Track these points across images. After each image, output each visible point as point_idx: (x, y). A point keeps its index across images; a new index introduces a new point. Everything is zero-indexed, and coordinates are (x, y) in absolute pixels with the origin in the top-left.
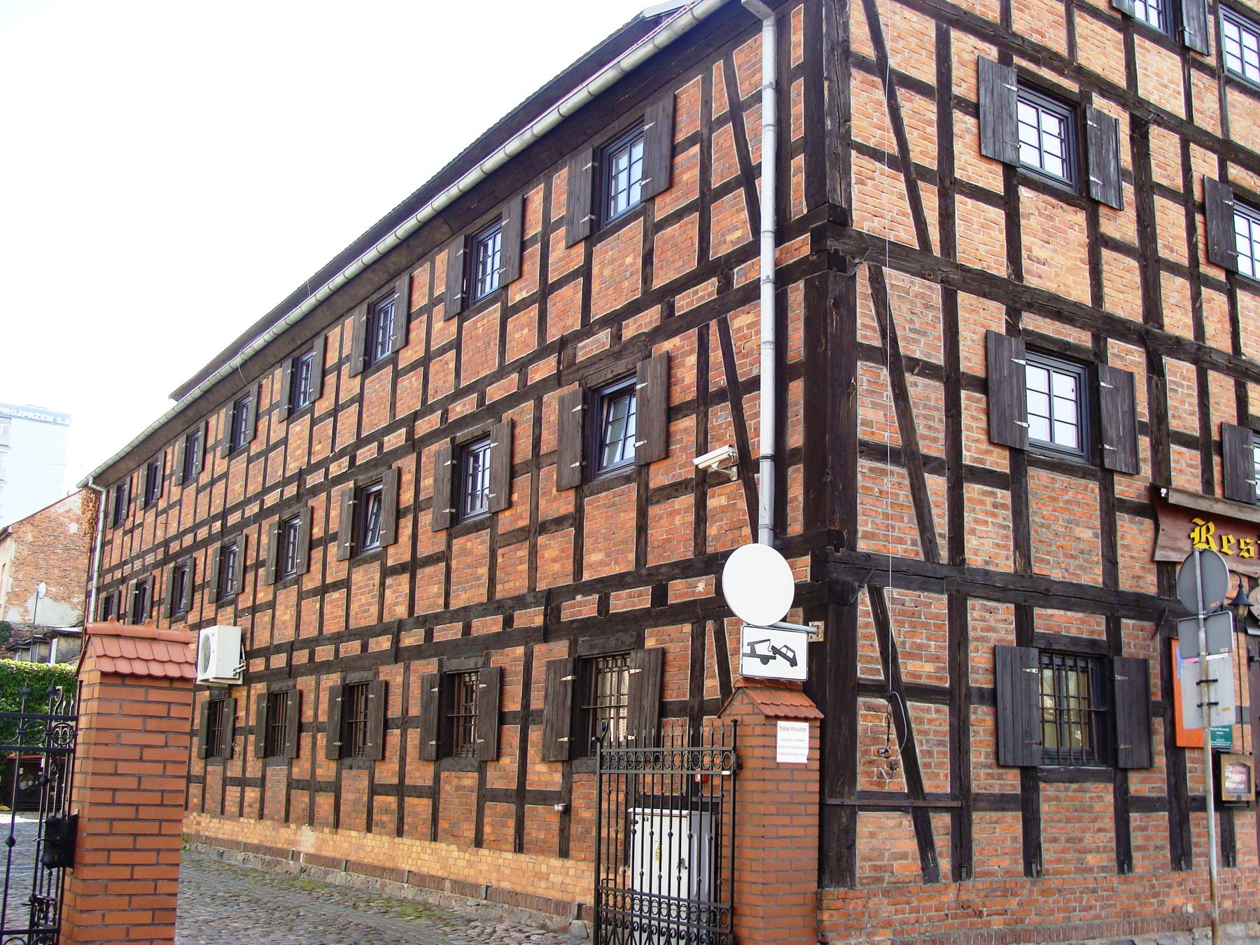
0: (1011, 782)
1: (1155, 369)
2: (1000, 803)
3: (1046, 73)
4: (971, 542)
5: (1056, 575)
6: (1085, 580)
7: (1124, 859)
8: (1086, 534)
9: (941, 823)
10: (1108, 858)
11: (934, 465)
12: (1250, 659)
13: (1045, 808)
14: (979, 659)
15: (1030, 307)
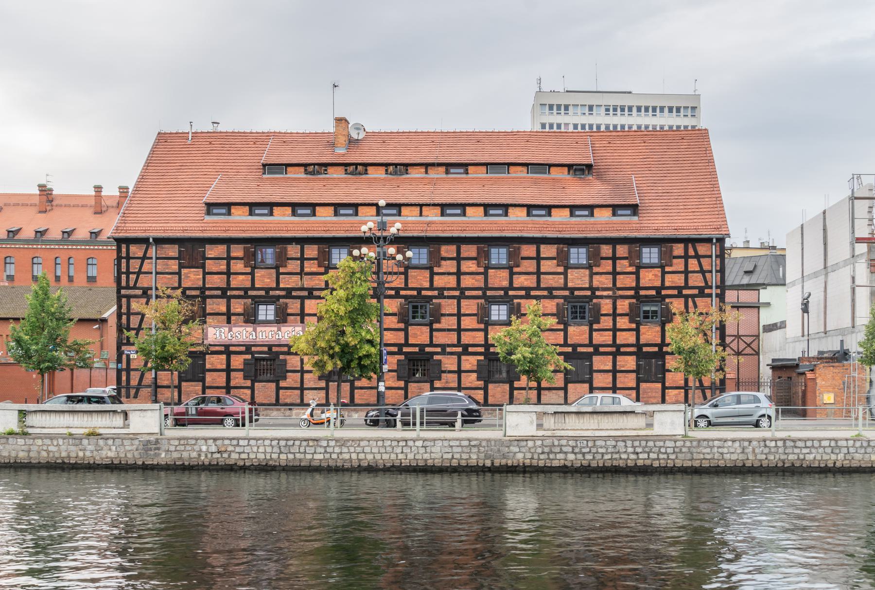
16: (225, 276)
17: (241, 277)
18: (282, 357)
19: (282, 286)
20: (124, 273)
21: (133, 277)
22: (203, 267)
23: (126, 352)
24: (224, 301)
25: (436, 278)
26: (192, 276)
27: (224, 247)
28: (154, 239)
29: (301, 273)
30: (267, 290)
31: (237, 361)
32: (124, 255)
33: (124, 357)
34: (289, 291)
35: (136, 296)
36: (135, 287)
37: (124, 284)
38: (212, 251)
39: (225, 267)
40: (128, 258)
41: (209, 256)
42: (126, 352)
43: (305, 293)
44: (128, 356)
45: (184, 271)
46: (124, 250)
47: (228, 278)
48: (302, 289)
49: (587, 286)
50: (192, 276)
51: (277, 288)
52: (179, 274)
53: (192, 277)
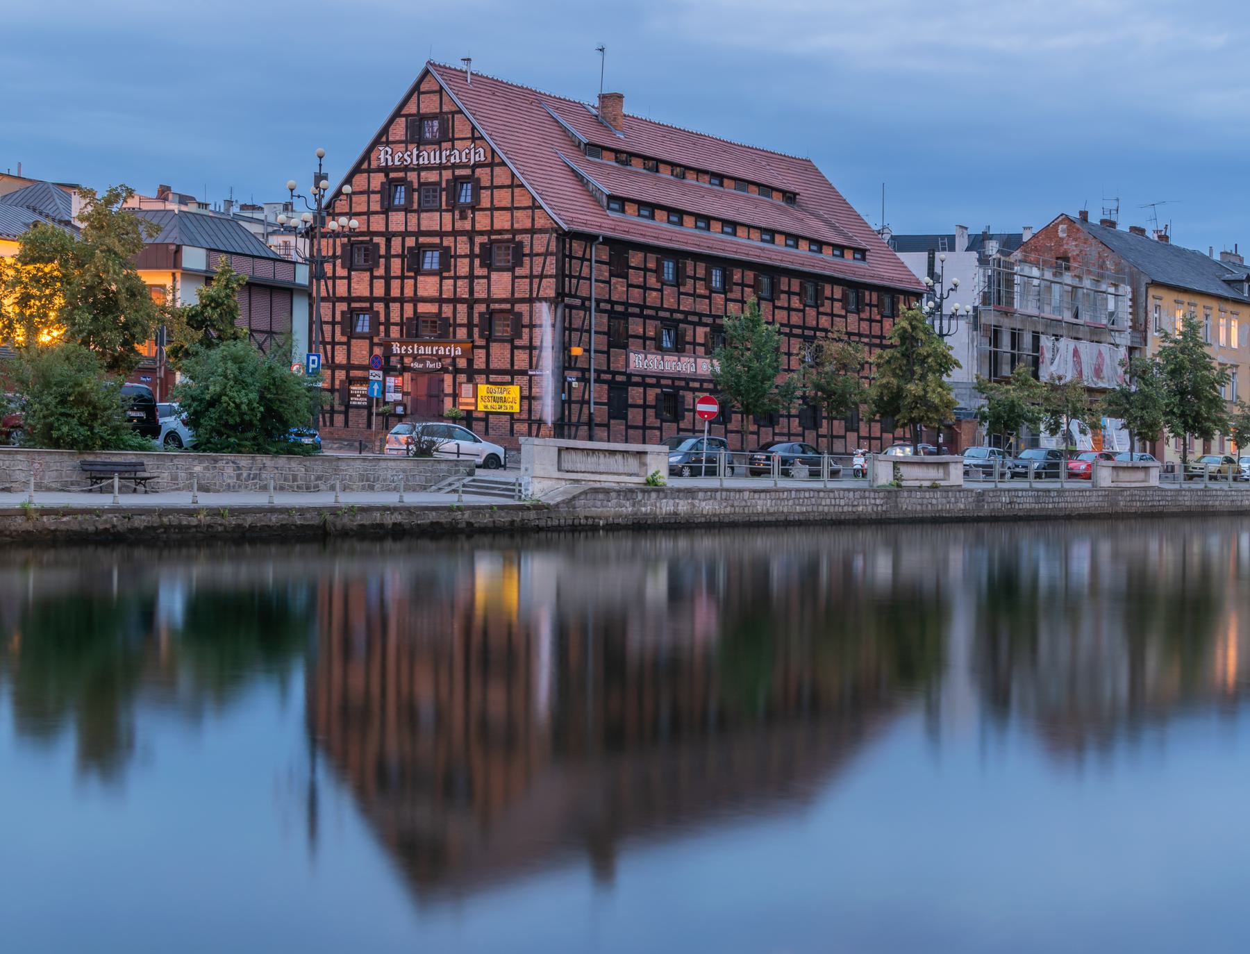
0: (343, 408)
1: (387, 307)
2: (340, 412)
3: (360, 238)
4: (336, 358)
5: (356, 363)
6: (364, 363)
7: (369, 425)
8: (364, 352)
9: (327, 416)
10: (365, 426)
11: (328, 343)
12: (412, 380)
13: (350, 414)
14: (337, 382)
15: (354, 302)
16: (642, 291)
17: (654, 294)
18: (681, 392)
19: (681, 308)
20: (567, 276)
21: (574, 281)
22: (626, 276)
23: (569, 379)
24: (640, 320)
25: (776, 311)
26: (620, 288)
27: (640, 255)
28: (604, 238)
29: (694, 295)
30: (672, 311)
31: (652, 394)
32: (567, 253)
33: (566, 384)
34: (686, 313)
35: (576, 307)
36: (575, 296)
37: (567, 290)
38: (635, 259)
39: (642, 279)
40: (571, 257)
41: (632, 265)
42: (569, 379)
43: (696, 319)
44: (570, 384)
45: (614, 280)
46: (568, 246)
47: (645, 293)
48: (694, 313)
49: (857, 331)
50: (620, 288)
51: (678, 311)
52: (609, 282)
53: (619, 286)
